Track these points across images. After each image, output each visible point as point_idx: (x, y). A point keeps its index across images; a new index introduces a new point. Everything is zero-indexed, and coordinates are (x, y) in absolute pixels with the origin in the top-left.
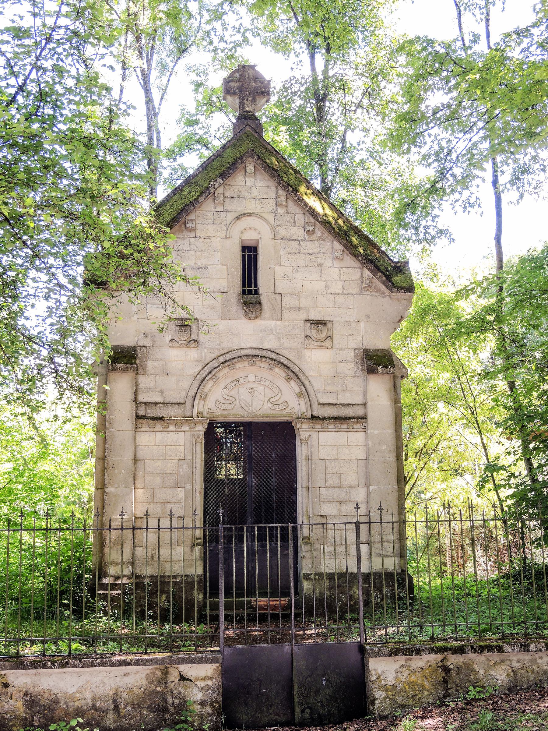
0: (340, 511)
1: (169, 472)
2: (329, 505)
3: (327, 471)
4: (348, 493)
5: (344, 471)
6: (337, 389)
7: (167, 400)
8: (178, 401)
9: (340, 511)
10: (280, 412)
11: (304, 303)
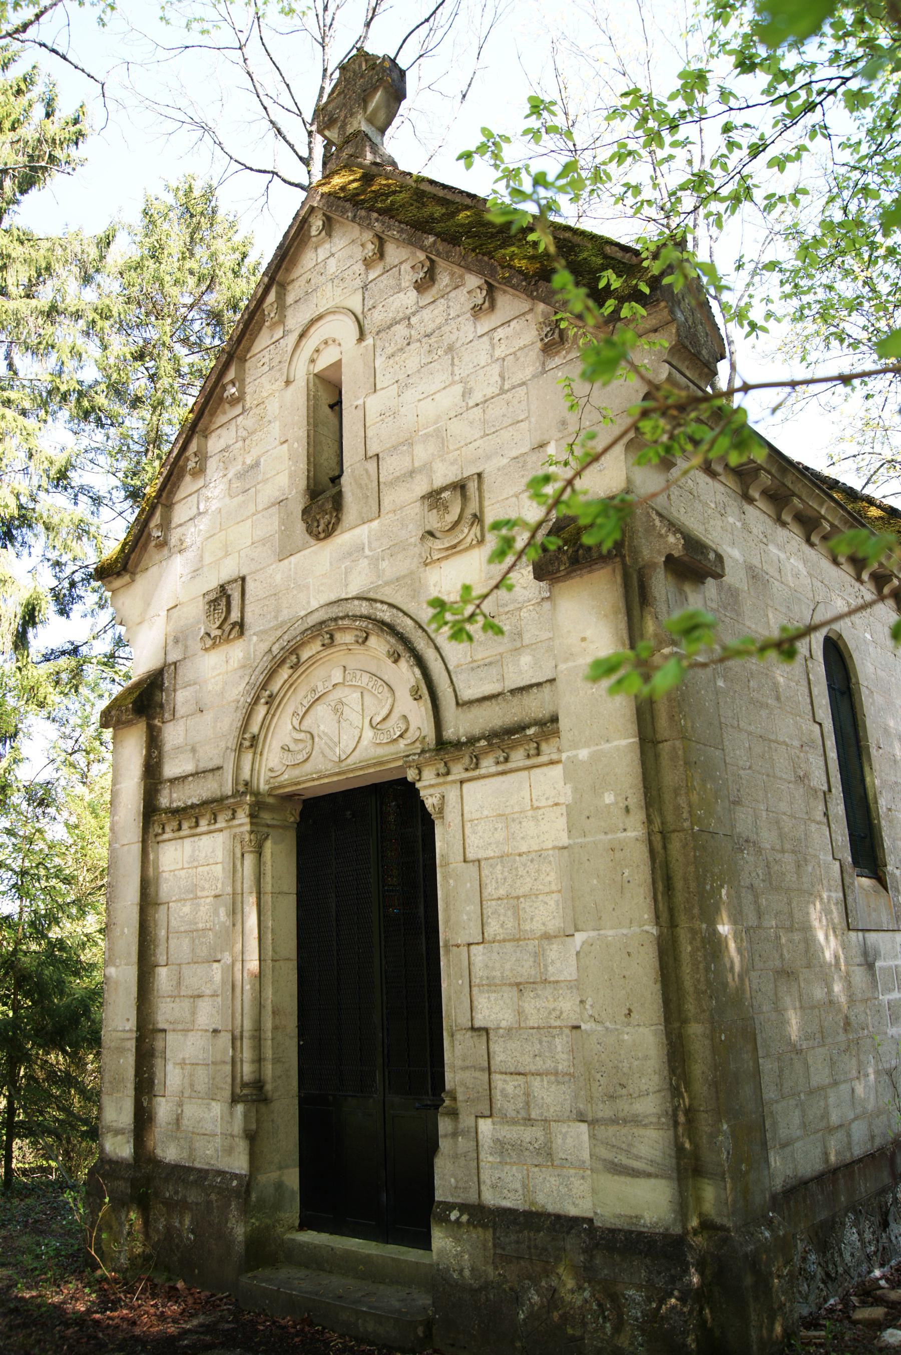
0: (520, 1012)
1: (201, 926)
2: (493, 996)
3: (485, 894)
4: (538, 956)
5: (525, 889)
6: (501, 649)
7: (203, 766)
8: (211, 765)
9: (520, 1012)
10: (392, 749)
11: (422, 453)
